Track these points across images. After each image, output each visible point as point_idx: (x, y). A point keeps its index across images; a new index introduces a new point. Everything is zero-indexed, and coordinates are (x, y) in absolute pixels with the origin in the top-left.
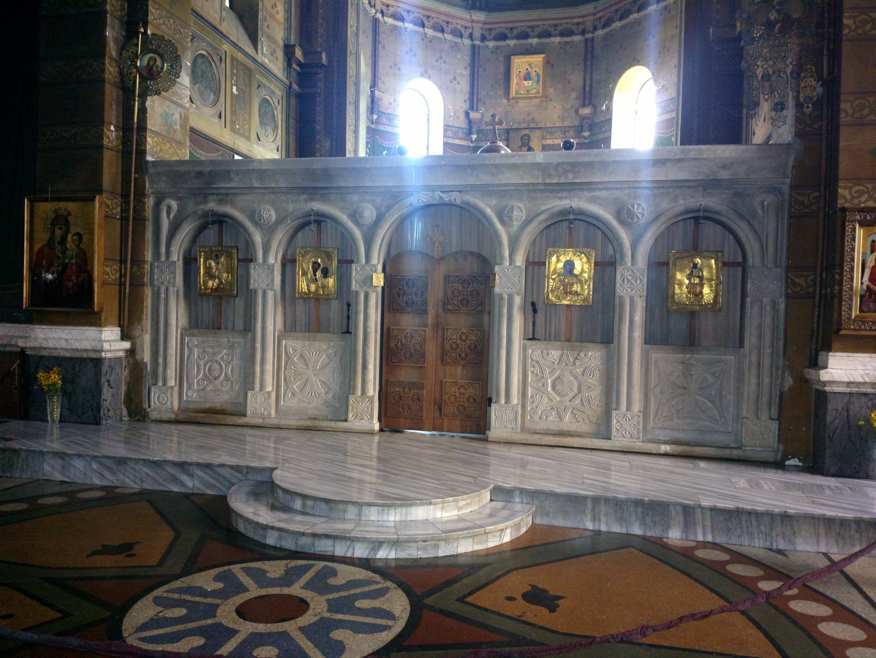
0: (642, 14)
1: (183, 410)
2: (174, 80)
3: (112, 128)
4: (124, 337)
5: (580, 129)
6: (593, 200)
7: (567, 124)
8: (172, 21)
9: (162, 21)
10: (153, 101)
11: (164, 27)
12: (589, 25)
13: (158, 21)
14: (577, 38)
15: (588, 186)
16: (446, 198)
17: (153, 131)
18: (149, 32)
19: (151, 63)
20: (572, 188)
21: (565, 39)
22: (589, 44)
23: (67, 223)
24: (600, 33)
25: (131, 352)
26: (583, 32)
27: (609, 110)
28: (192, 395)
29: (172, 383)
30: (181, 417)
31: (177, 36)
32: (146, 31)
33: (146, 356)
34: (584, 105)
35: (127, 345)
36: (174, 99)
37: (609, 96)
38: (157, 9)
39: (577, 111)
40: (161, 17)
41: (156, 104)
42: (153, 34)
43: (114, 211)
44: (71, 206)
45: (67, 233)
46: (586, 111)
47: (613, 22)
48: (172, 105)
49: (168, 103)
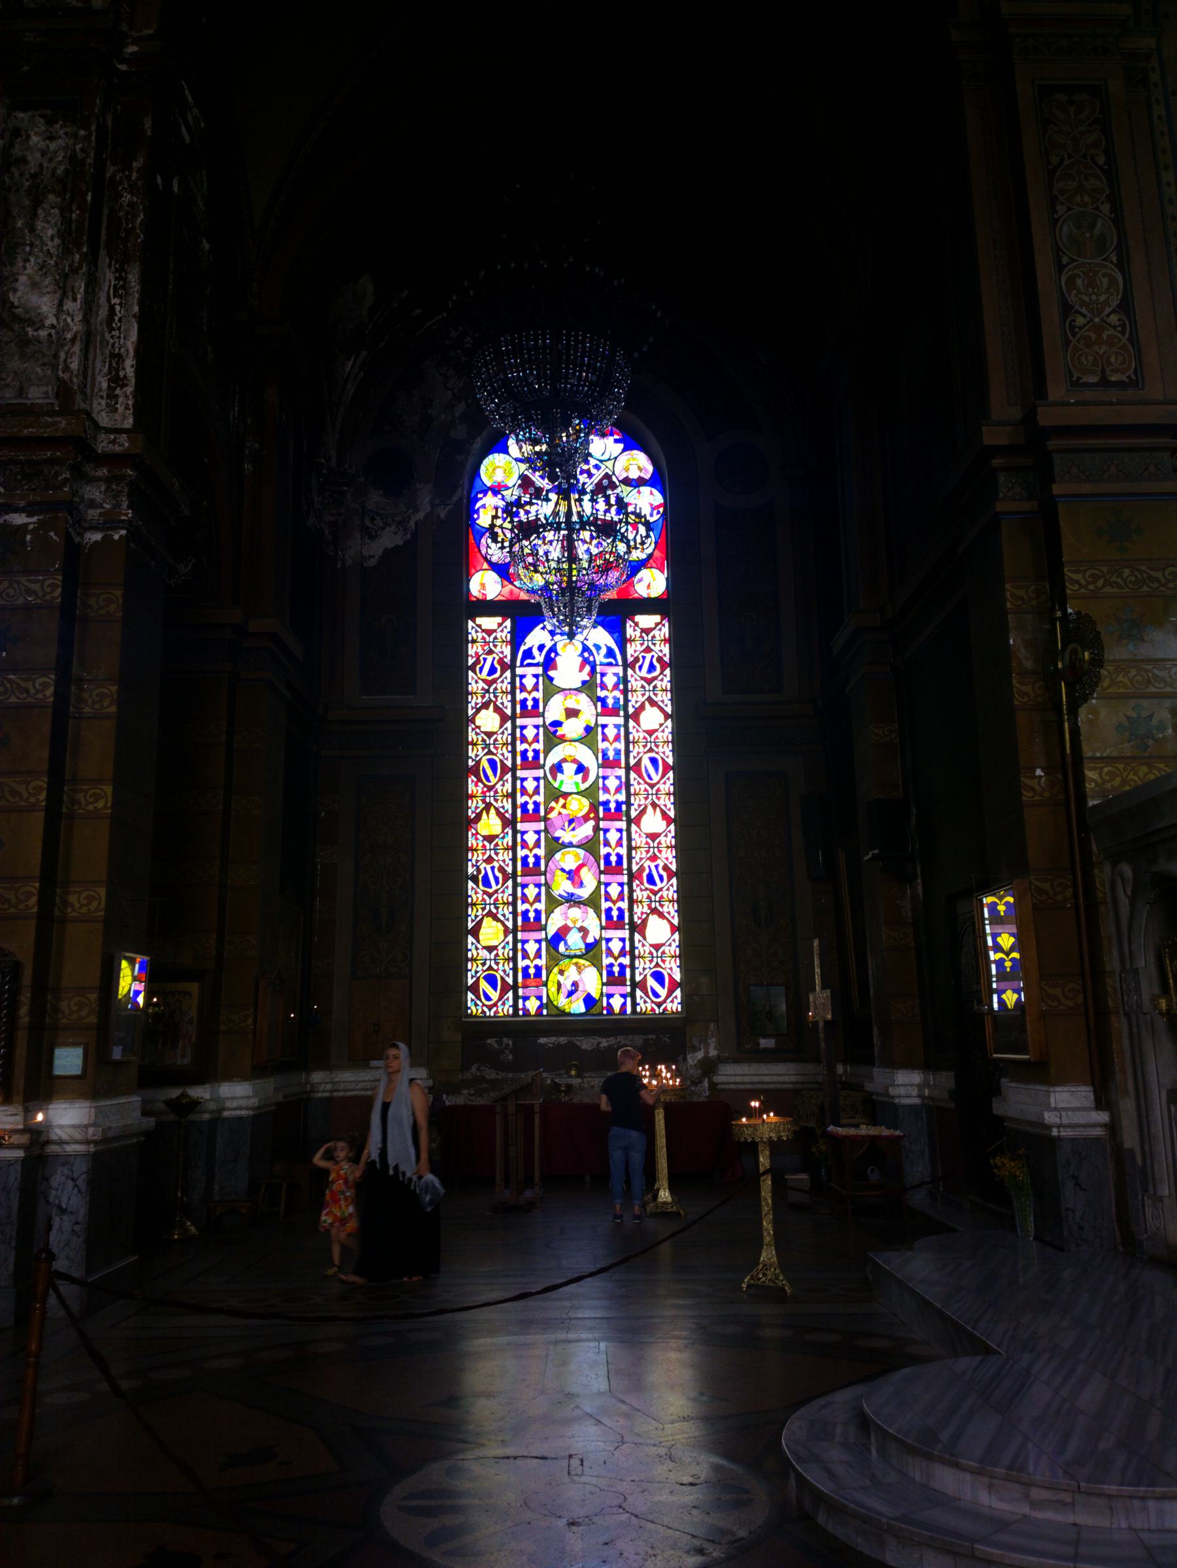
2: (1099, 672)
3: (1039, 772)
4: (1099, 1105)
8: (1127, 572)
9: (1100, 583)
10: (1094, 711)
11: (1108, 589)
13: (1091, 587)
17: (1102, 758)
18: (1070, 611)
19: (1074, 657)
31: (1145, 589)
32: (1064, 611)
33: (1130, 1140)
35: (1103, 1117)
36: (1152, 689)
38: (1084, 572)
40: (1095, 578)
41: (1103, 713)
42: (1078, 613)
43: (1059, 898)
48: (1145, 703)
49: (1133, 702)
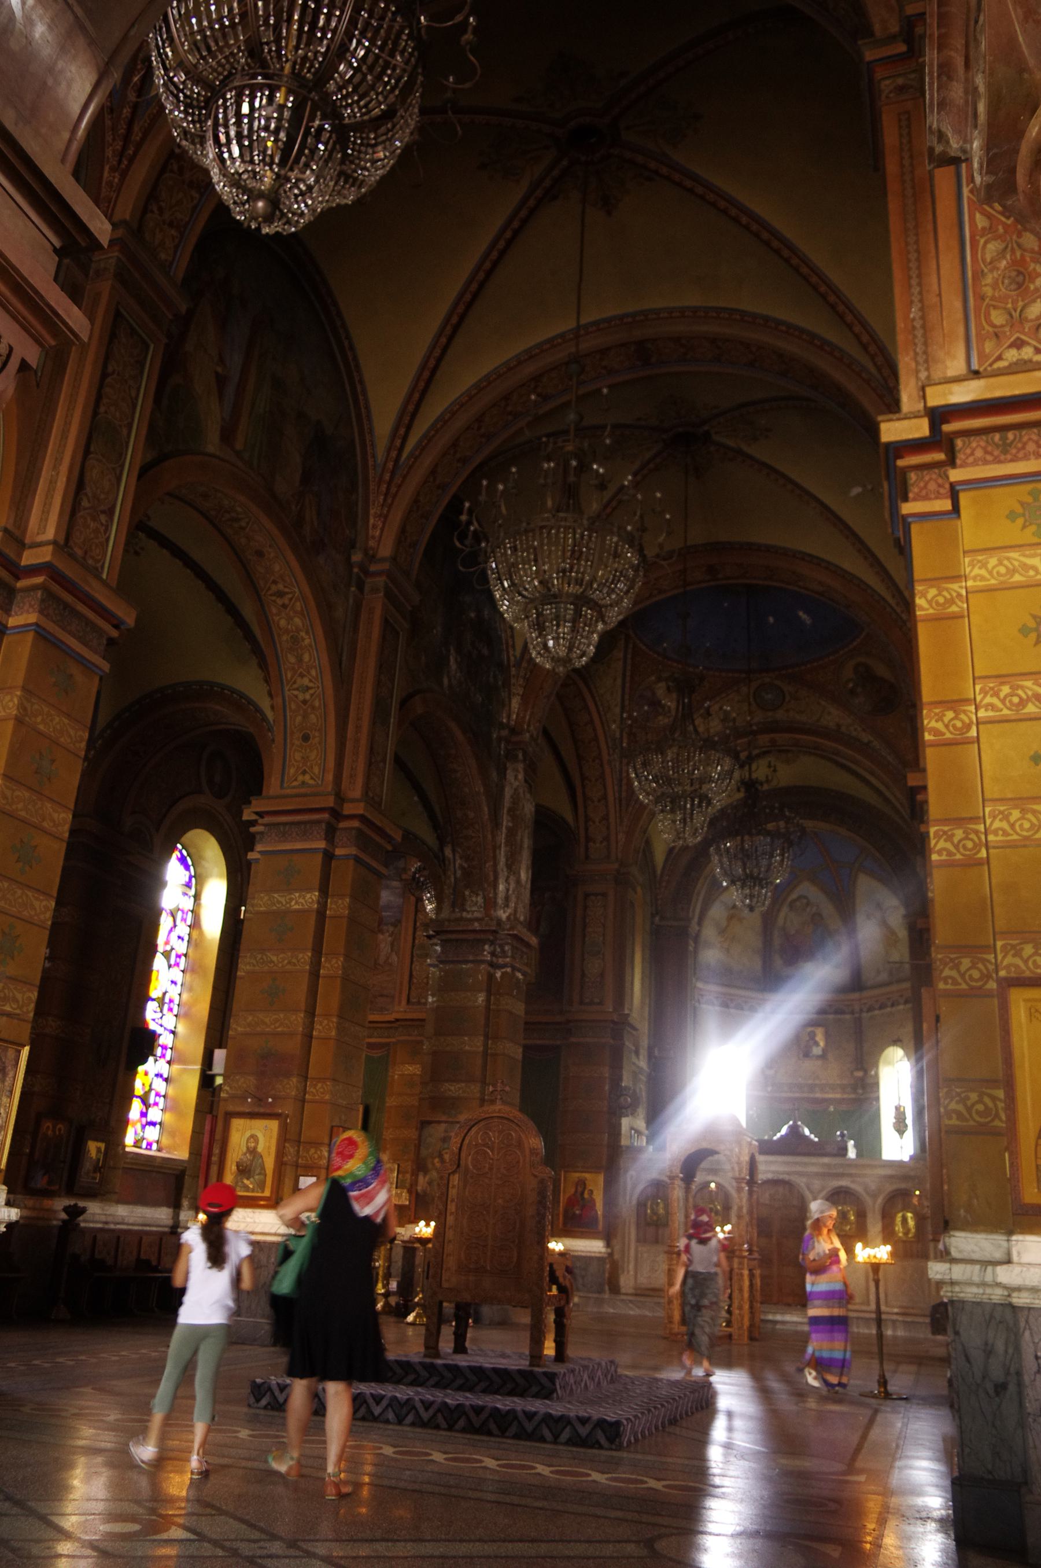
0: (894, 1009)
1: (635, 1289)
5: (854, 1088)
6: (853, 1182)
7: (845, 1082)
12: (857, 1008)
14: (848, 1017)
15: (850, 1175)
16: (781, 1177)
20: (842, 1175)
21: (839, 1016)
22: (858, 1022)
23: (585, 1184)
24: (864, 1015)
25: (611, 1255)
26: (852, 1013)
27: (877, 1076)
28: (643, 1281)
29: (632, 1273)
30: (639, 1292)
34: (857, 1069)
37: (876, 1065)
39: (852, 1073)
44: (587, 1176)
45: (585, 1188)
46: (860, 1074)
47: (874, 1009)
